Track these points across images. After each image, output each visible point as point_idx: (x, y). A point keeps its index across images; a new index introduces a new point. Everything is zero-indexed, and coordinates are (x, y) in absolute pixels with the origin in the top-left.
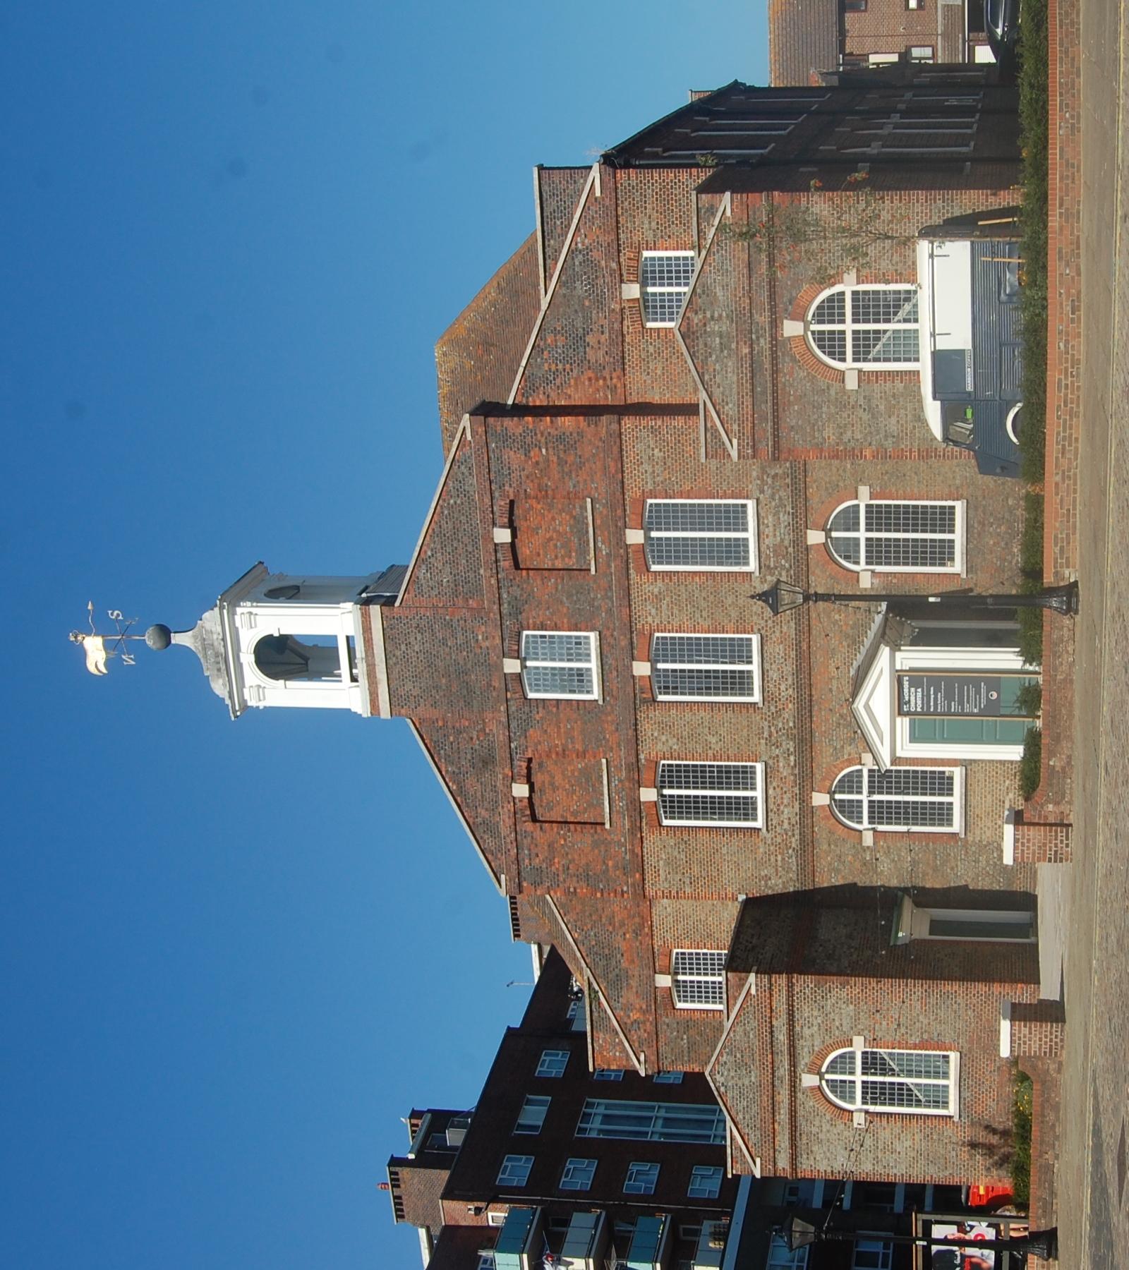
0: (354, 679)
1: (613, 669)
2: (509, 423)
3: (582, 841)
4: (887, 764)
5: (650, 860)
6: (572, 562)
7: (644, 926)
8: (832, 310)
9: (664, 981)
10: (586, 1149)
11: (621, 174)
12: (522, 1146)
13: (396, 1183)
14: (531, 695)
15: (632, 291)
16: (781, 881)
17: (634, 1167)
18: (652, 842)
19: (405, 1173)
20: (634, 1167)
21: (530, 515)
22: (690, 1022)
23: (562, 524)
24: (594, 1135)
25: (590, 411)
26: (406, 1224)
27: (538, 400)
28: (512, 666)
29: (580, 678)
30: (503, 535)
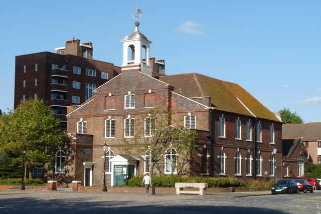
0: (128, 63)
1: (129, 111)
2: (167, 93)
3: (102, 106)
4: (110, 160)
5: (99, 118)
6: (146, 104)
7: (90, 116)
8: (173, 152)
9: (81, 120)
10: (83, 86)
11: (208, 112)
12: (83, 71)
13: (74, 41)
14: (125, 96)
15: (189, 114)
16: (96, 141)
17: (79, 98)
18: (102, 118)
19: (75, 45)
20: (79, 98)
21: (153, 97)
22: (75, 125)
23: (152, 102)
24: (86, 87)
25: (170, 107)
26: (65, 44)
27: (172, 97)
28: (129, 93)
29: (128, 105)
30: (150, 91)
